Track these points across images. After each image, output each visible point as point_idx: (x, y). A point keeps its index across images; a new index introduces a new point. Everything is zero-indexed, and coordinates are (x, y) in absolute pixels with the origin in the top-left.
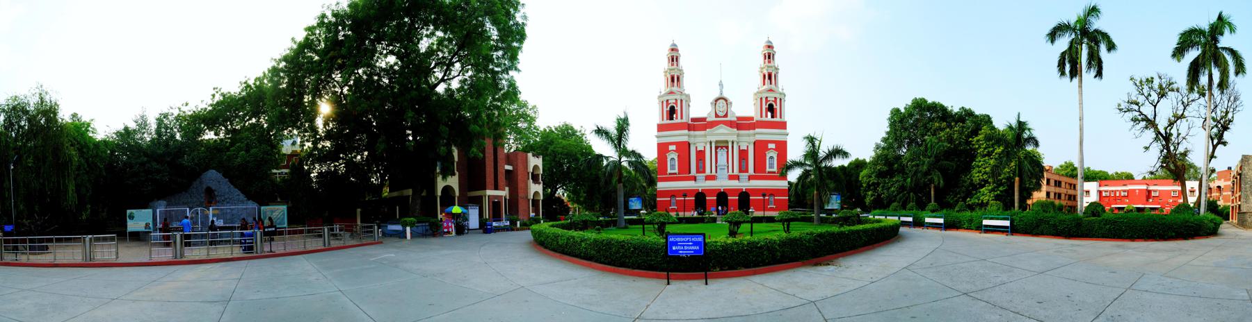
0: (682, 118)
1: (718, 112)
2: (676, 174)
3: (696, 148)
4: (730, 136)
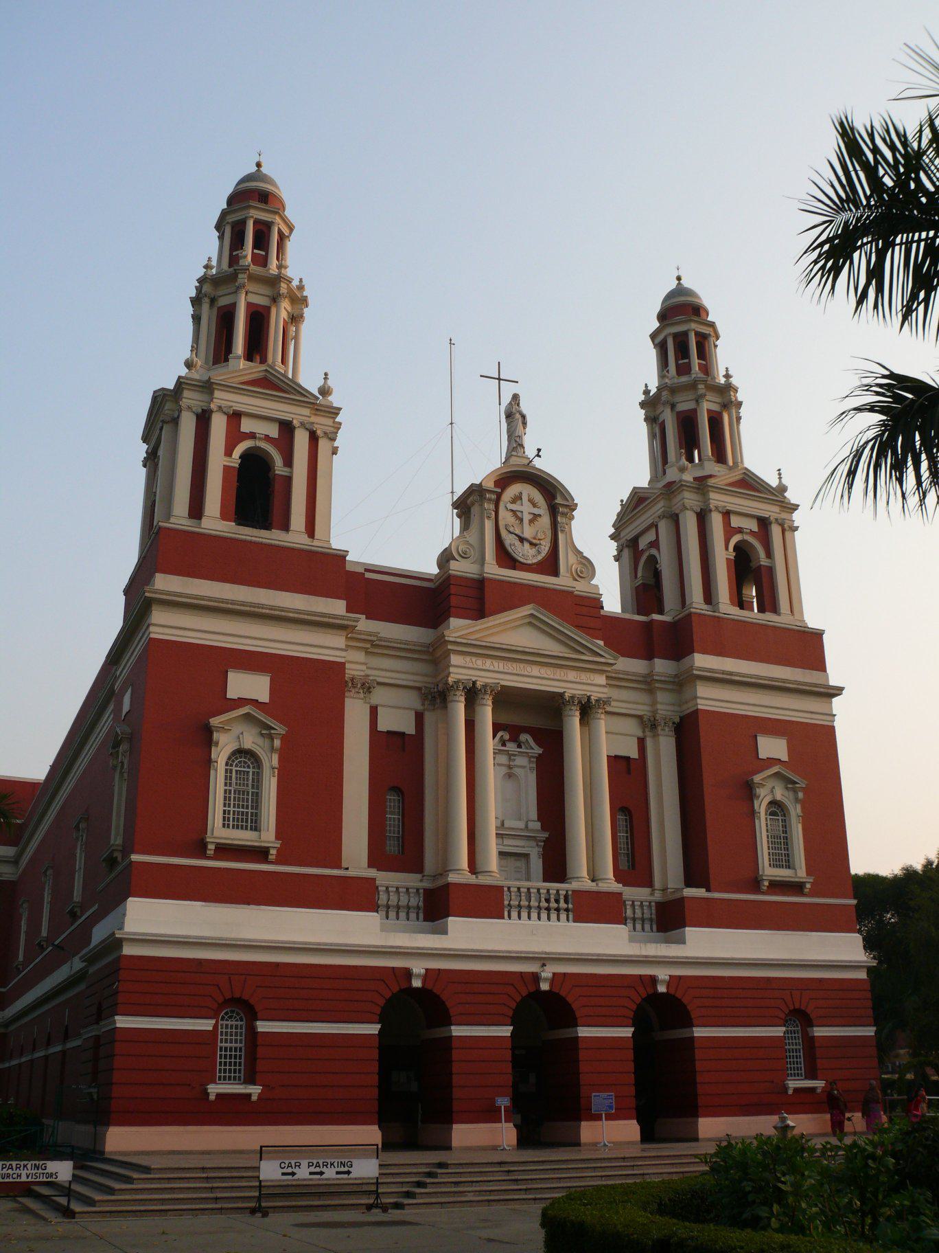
1: (509, 540)
2: (260, 854)
3: (374, 711)
4: (572, 675)
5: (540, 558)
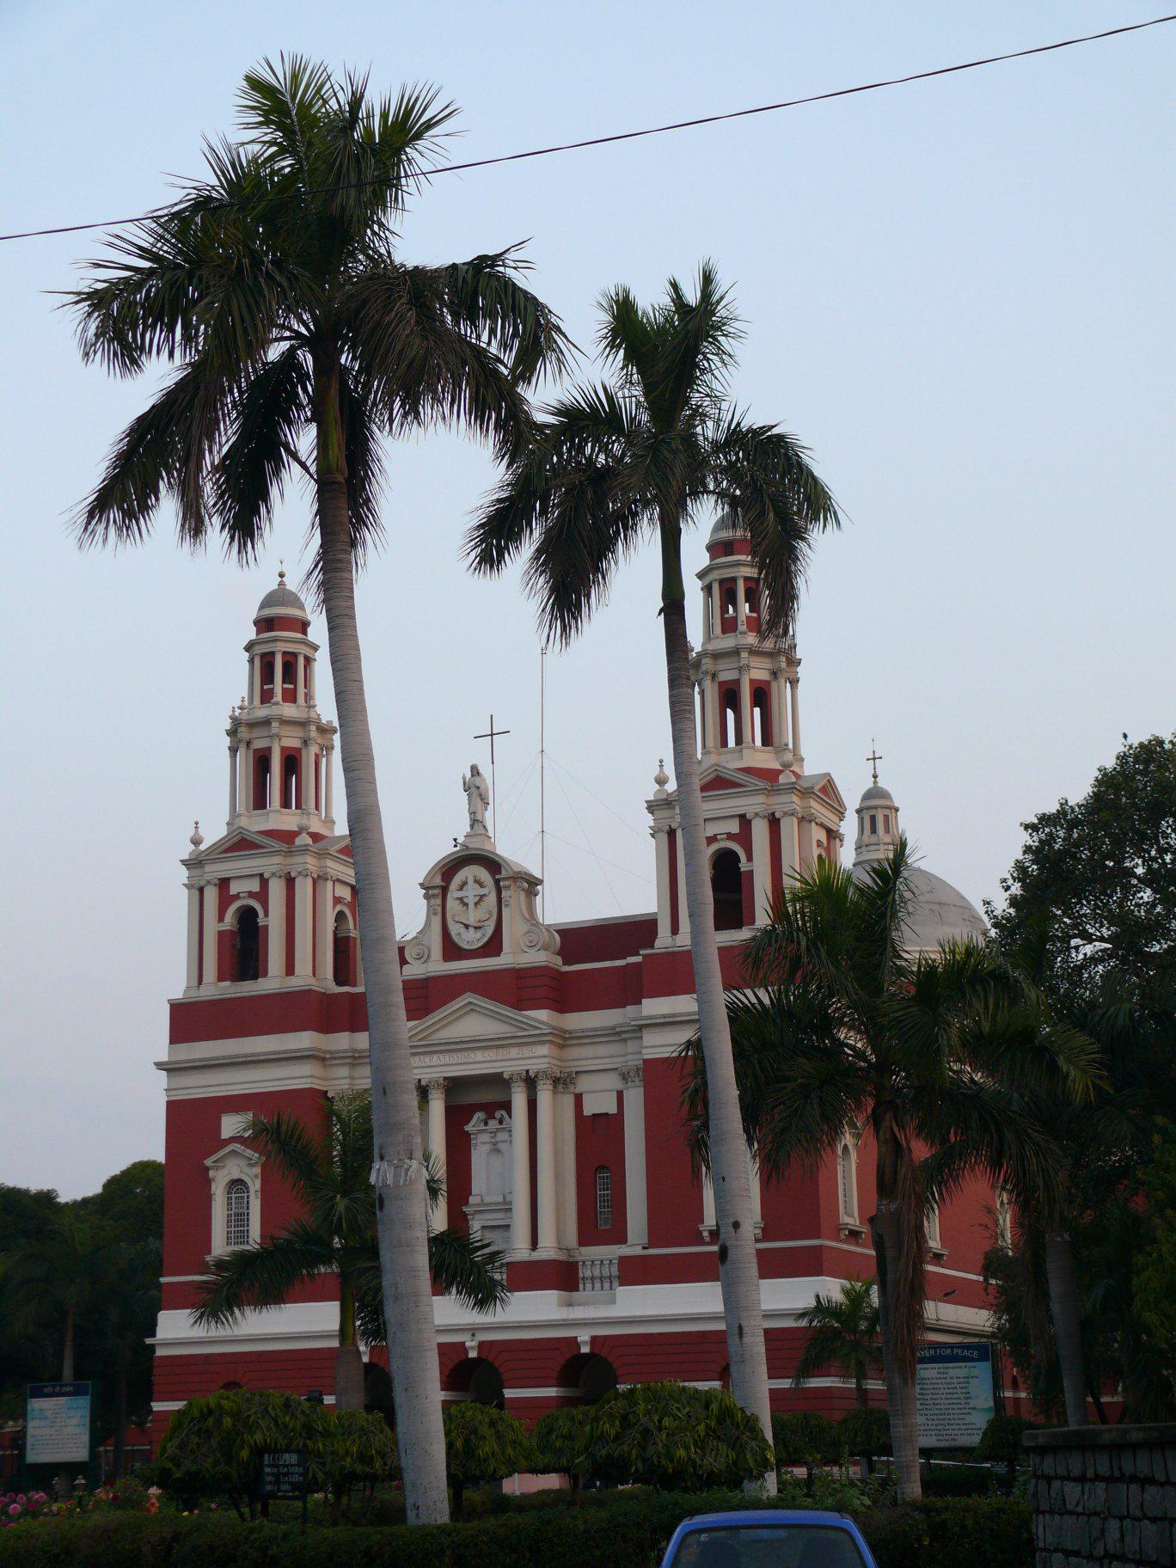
0: (290, 970)
1: (454, 929)
4: (514, 1052)
5: (485, 940)
